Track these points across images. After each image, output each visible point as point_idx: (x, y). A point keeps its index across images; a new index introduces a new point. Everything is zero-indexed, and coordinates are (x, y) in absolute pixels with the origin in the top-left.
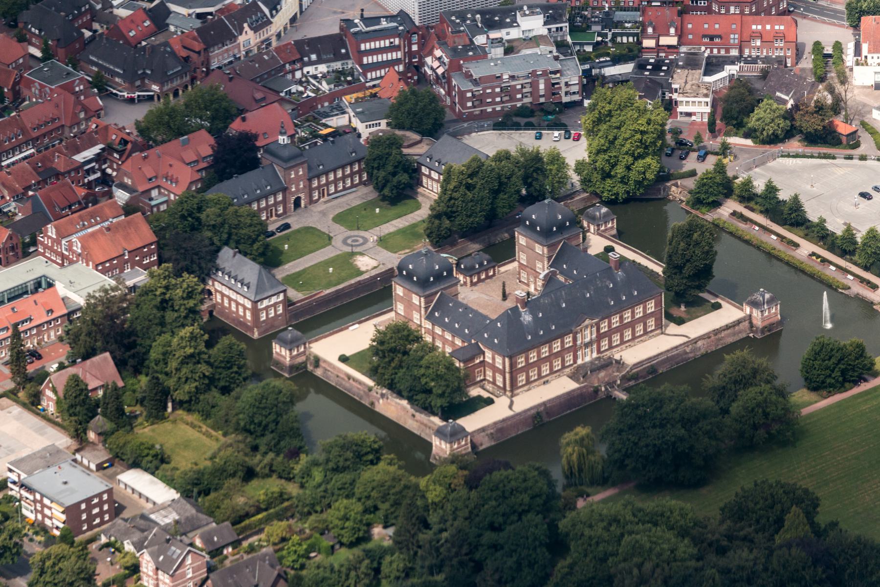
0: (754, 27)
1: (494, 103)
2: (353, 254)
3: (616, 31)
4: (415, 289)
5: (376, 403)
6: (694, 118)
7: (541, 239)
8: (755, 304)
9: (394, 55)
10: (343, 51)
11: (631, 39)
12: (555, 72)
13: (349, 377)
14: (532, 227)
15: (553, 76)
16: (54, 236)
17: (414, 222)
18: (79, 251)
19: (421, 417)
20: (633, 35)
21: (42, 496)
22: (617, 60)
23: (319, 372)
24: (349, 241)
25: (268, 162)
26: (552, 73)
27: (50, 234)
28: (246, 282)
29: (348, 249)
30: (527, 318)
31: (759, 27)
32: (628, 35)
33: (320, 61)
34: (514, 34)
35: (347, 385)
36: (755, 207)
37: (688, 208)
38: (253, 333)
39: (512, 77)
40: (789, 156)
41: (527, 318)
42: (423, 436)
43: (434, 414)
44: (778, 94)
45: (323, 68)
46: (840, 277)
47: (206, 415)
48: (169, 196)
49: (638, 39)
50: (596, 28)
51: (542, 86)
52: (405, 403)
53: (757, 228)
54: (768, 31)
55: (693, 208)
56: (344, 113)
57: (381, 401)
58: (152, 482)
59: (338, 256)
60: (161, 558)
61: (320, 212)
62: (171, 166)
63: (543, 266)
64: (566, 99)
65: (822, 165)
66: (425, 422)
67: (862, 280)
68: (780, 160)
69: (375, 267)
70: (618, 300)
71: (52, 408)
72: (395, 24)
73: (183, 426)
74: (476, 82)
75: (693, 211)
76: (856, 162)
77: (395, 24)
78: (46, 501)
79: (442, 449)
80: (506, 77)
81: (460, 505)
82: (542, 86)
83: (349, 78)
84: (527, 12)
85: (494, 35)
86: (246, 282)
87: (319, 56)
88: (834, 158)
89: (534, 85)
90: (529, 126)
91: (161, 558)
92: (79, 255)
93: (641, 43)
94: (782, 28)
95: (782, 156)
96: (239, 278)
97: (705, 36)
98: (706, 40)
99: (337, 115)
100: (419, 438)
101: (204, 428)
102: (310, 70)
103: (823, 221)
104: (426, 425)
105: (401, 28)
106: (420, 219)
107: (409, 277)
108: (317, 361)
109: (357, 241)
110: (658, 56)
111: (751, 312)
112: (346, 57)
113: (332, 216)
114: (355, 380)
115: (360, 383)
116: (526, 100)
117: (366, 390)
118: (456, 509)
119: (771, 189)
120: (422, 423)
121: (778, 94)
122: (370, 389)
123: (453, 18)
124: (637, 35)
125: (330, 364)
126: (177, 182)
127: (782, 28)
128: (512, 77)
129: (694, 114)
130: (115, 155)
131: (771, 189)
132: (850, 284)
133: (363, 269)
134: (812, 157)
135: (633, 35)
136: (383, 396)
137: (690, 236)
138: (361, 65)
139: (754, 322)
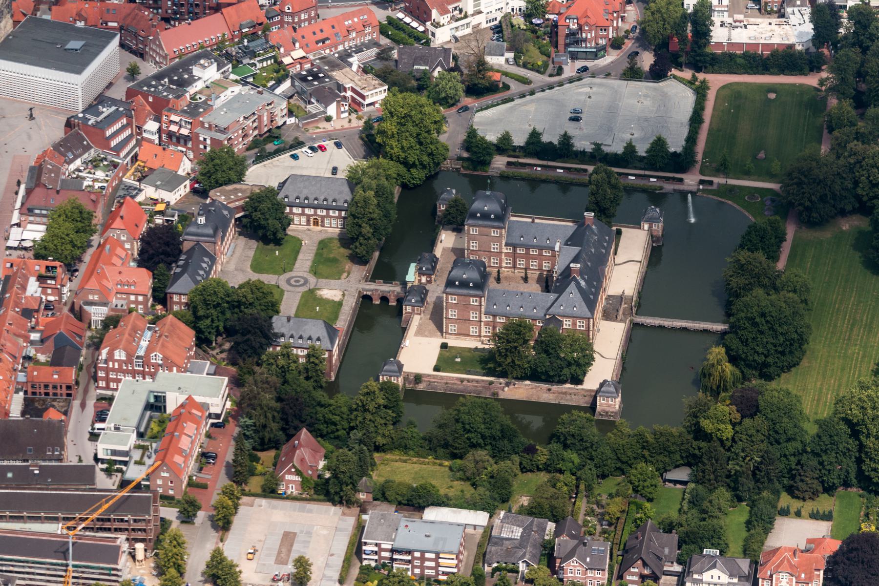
0: (346, 23)
1: (239, 144)
2: (312, 291)
3: (259, 59)
4: (472, 292)
5: (500, 392)
6: (377, 105)
7: (496, 224)
8: (651, 221)
9: (128, 132)
10: (85, 143)
11: (269, 62)
12: (270, 104)
13: (462, 380)
14: (485, 216)
15: (270, 107)
16: (124, 358)
17: (314, 252)
18: (160, 362)
19: (555, 388)
20: (270, 58)
21: (423, 552)
22: (279, 82)
23: (421, 387)
24: (292, 282)
25: (192, 244)
26: (268, 105)
27: (117, 357)
28: (314, 337)
29: (305, 289)
30: (583, 283)
31: (350, 22)
32: (266, 59)
33: (76, 157)
34: (199, 86)
35: (460, 387)
36: (517, 154)
37: (468, 172)
38: (330, 377)
39: (245, 118)
40: (482, 110)
41: (583, 283)
42: (562, 402)
43: (565, 382)
44: (416, 67)
45: (78, 163)
46: (641, 183)
47: (404, 448)
48: (128, 298)
49: (276, 61)
50: (246, 61)
51: (265, 118)
52: (528, 382)
53: (539, 169)
54: (358, 23)
55: (475, 169)
56: (140, 190)
57: (506, 389)
58: (454, 512)
59: (302, 297)
60: (588, 559)
61: (236, 269)
62: (120, 273)
63: (501, 246)
64: (280, 124)
65: (512, 107)
66: (564, 390)
67: (667, 179)
68: (478, 114)
69: (344, 295)
70: (604, 248)
71: (293, 490)
72: (114, 108)
73: (397, 464)
74: (224, 131)
75: (476, 173)
76: (528, 98)
77: (114, 108)
78: (427, 555)
79: (609, 405)
80: (242, 119)
81: (753, 432)
82: (265, 118)
83: (106, 163)
84: (206, 65)
85: (192, 90)
86: (314, 337)
87: (73, 153)
88: (513, 100)
89: (260, 118)
90: (278, 152)
91: (588, 559)
92: (161, 366)
93: (282, 62)
94: (365, 17)
95: (478, 111)
96: (306, 336)
97: (317, 43)
98: (320, 44)
99: (137, 194)
100: (559, 405)
101: (415, 459)
102: (72, 167)
103: (598, 146)
104: (565, 393)
105: (121, 109)
106: (315, 248)
107: (464, 284)
108: (418, 378)
109: (296, 281)
110: (597, 44)
111: (650, 227)
112: (87, 148)
113: (249, 270)
114: (468, 380)
115: (477, 381)
116: (256, 132)
117: (487, 385)
118: (751, 436)
119: (535, 135)
120: (562, 393)
121: (416, 67)
122: (491, 383)
123: (145, 88)
124: (274, 57)
125: (429, 375)
126: (134, 284)
127: (365, 17)
128: (245, 118)
129: (376, 102)
130: (49, 282)
131: (535, 135)
132: (658, 184)
133: (337, 299)
134: (498, 104)
135: (270, 58)
136: (507, 384)
137: (609, 182)
138: (111, 149)
139: (655, 234)
